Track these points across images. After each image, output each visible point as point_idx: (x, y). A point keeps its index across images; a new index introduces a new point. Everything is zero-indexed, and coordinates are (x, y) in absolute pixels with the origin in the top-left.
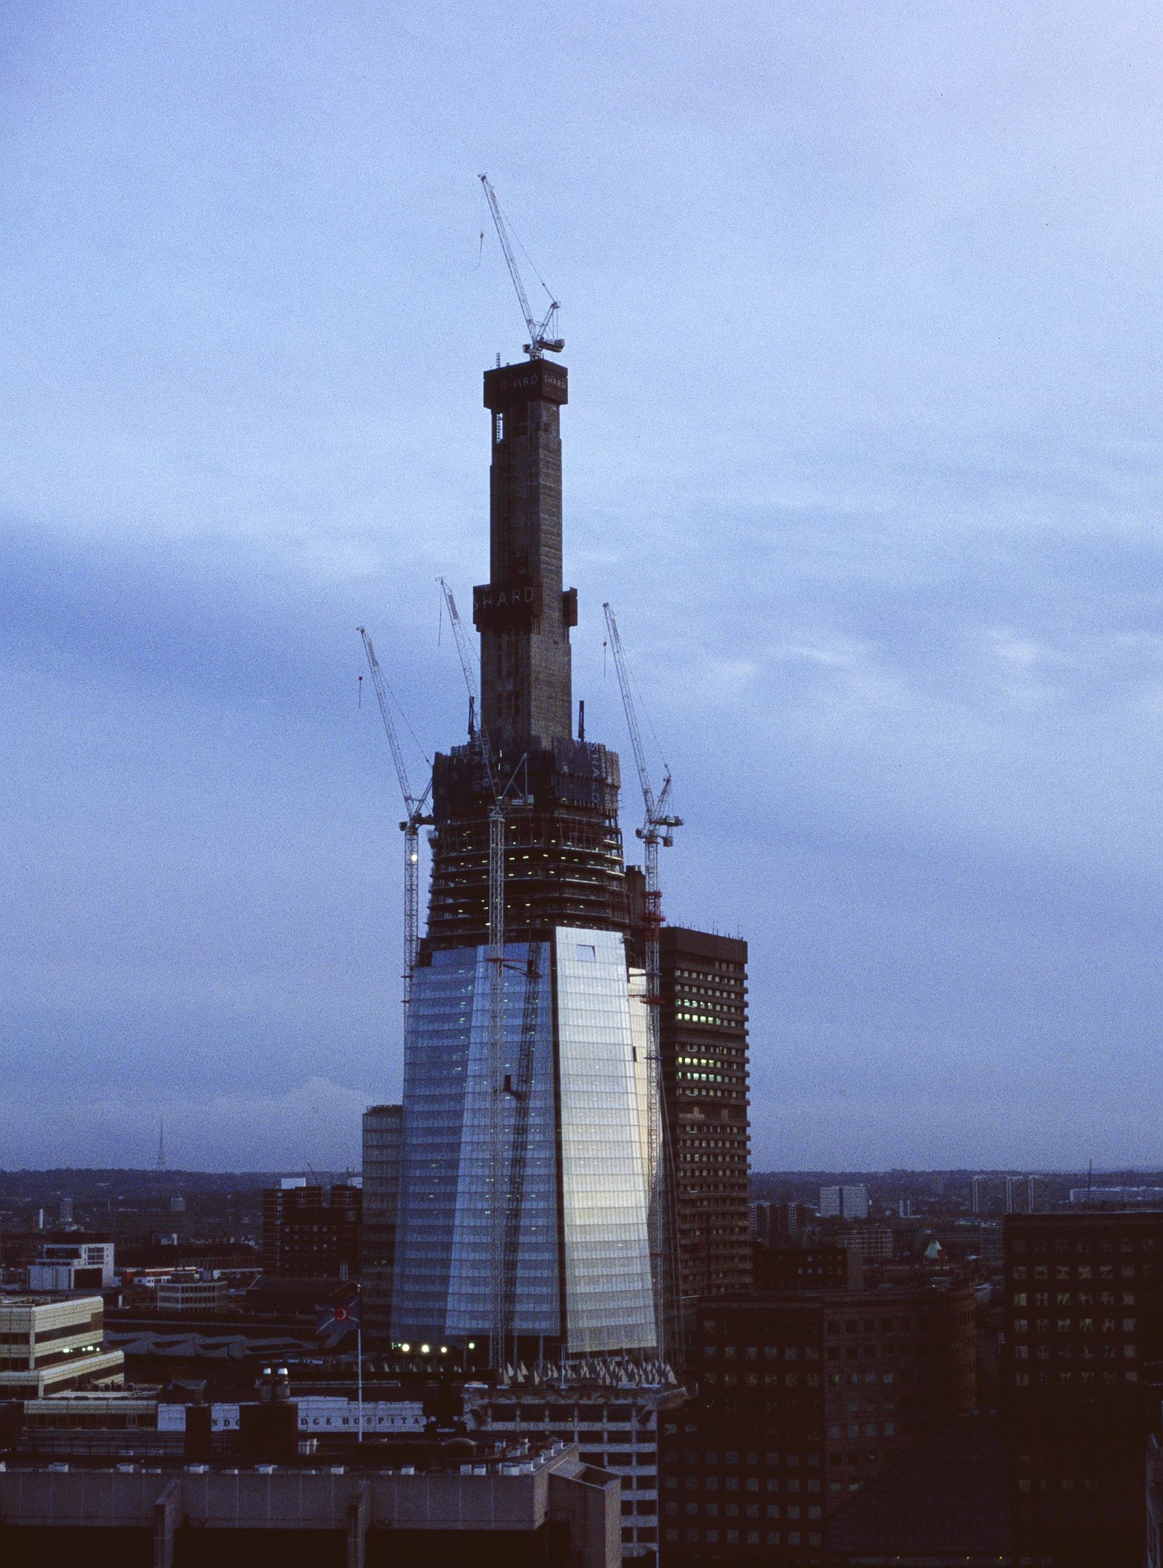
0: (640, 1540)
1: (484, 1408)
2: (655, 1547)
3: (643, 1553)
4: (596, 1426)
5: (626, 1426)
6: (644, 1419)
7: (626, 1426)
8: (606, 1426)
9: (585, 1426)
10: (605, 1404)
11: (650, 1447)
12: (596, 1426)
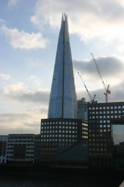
0: (31, 158)
1: (10, 137)
2: (33, 159)
3: (31, 160)
4: (25, 140)
5: (29, 140)
6: (32, 139)
7: (29, 140)
8: (27, 140)
9: (24, 140)
10: (27, 136)
11: (33, 143)
12: (25, 140)
